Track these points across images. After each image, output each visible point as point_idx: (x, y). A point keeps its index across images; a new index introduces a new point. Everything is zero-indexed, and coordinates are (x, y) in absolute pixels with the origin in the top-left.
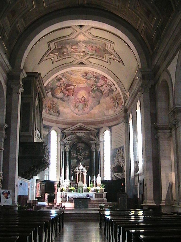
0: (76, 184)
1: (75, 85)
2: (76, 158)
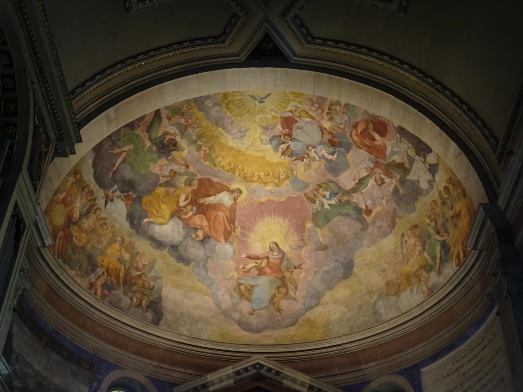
1: (241, 192)
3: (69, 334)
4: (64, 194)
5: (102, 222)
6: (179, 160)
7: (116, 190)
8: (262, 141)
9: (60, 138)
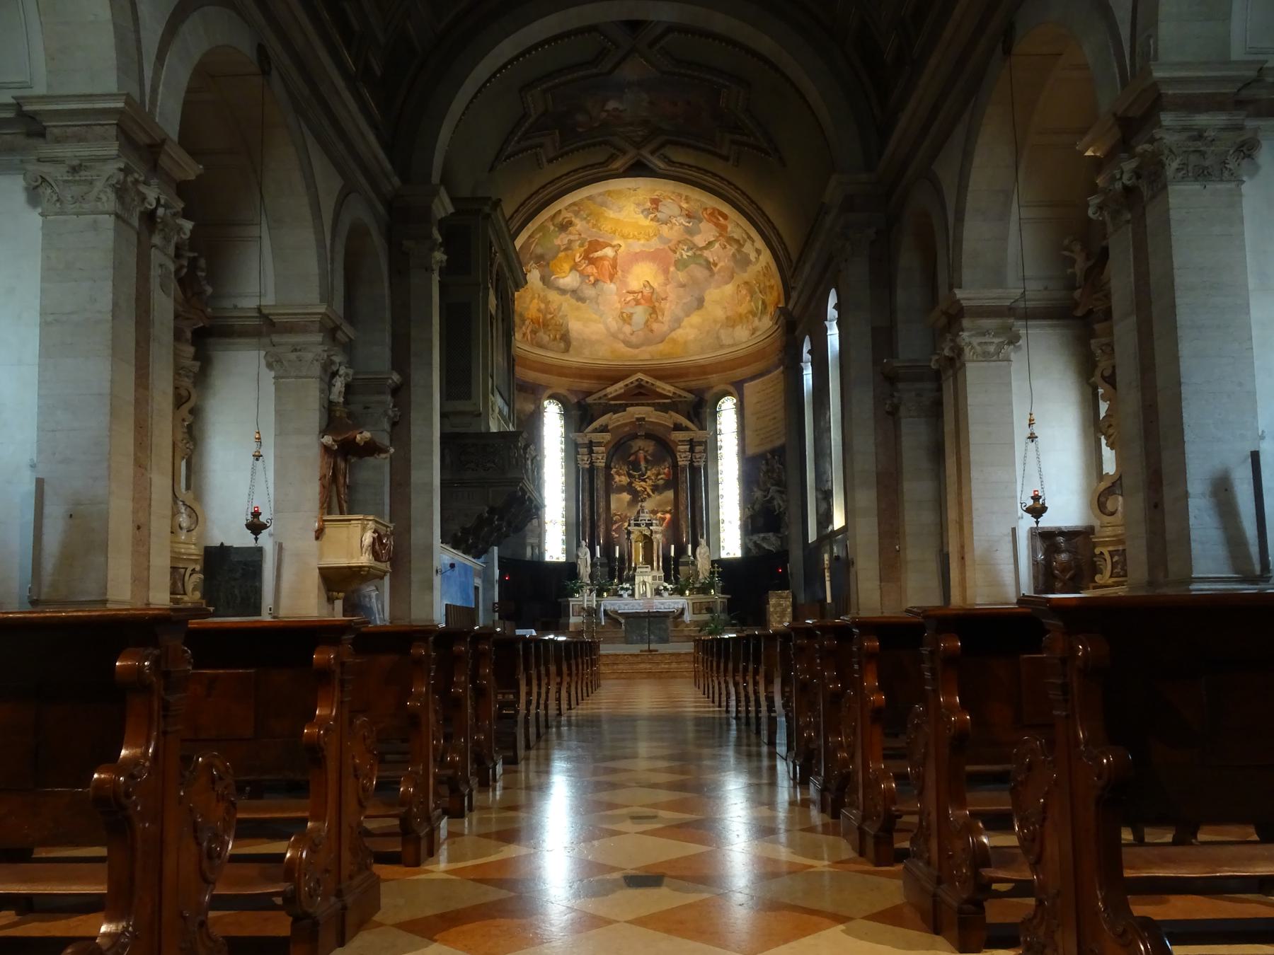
0: (630, 570)
1: (620, 246)
2: (629, 488)
8: (635, 213)
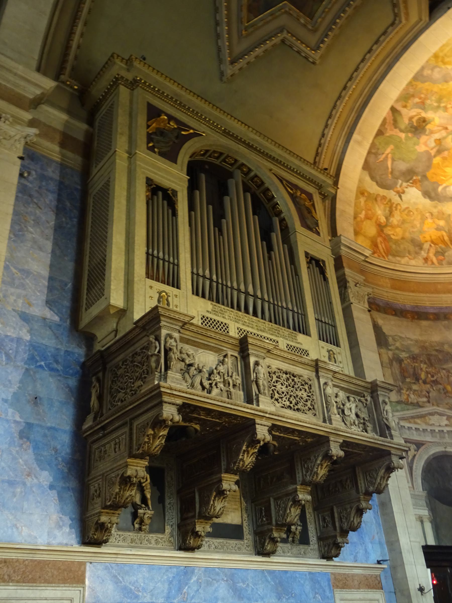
3: (427, 303)
4: (364, 212)
5: (407, 211)
6: (436, 128)
7: (402, 184)
9: (319, 187)
